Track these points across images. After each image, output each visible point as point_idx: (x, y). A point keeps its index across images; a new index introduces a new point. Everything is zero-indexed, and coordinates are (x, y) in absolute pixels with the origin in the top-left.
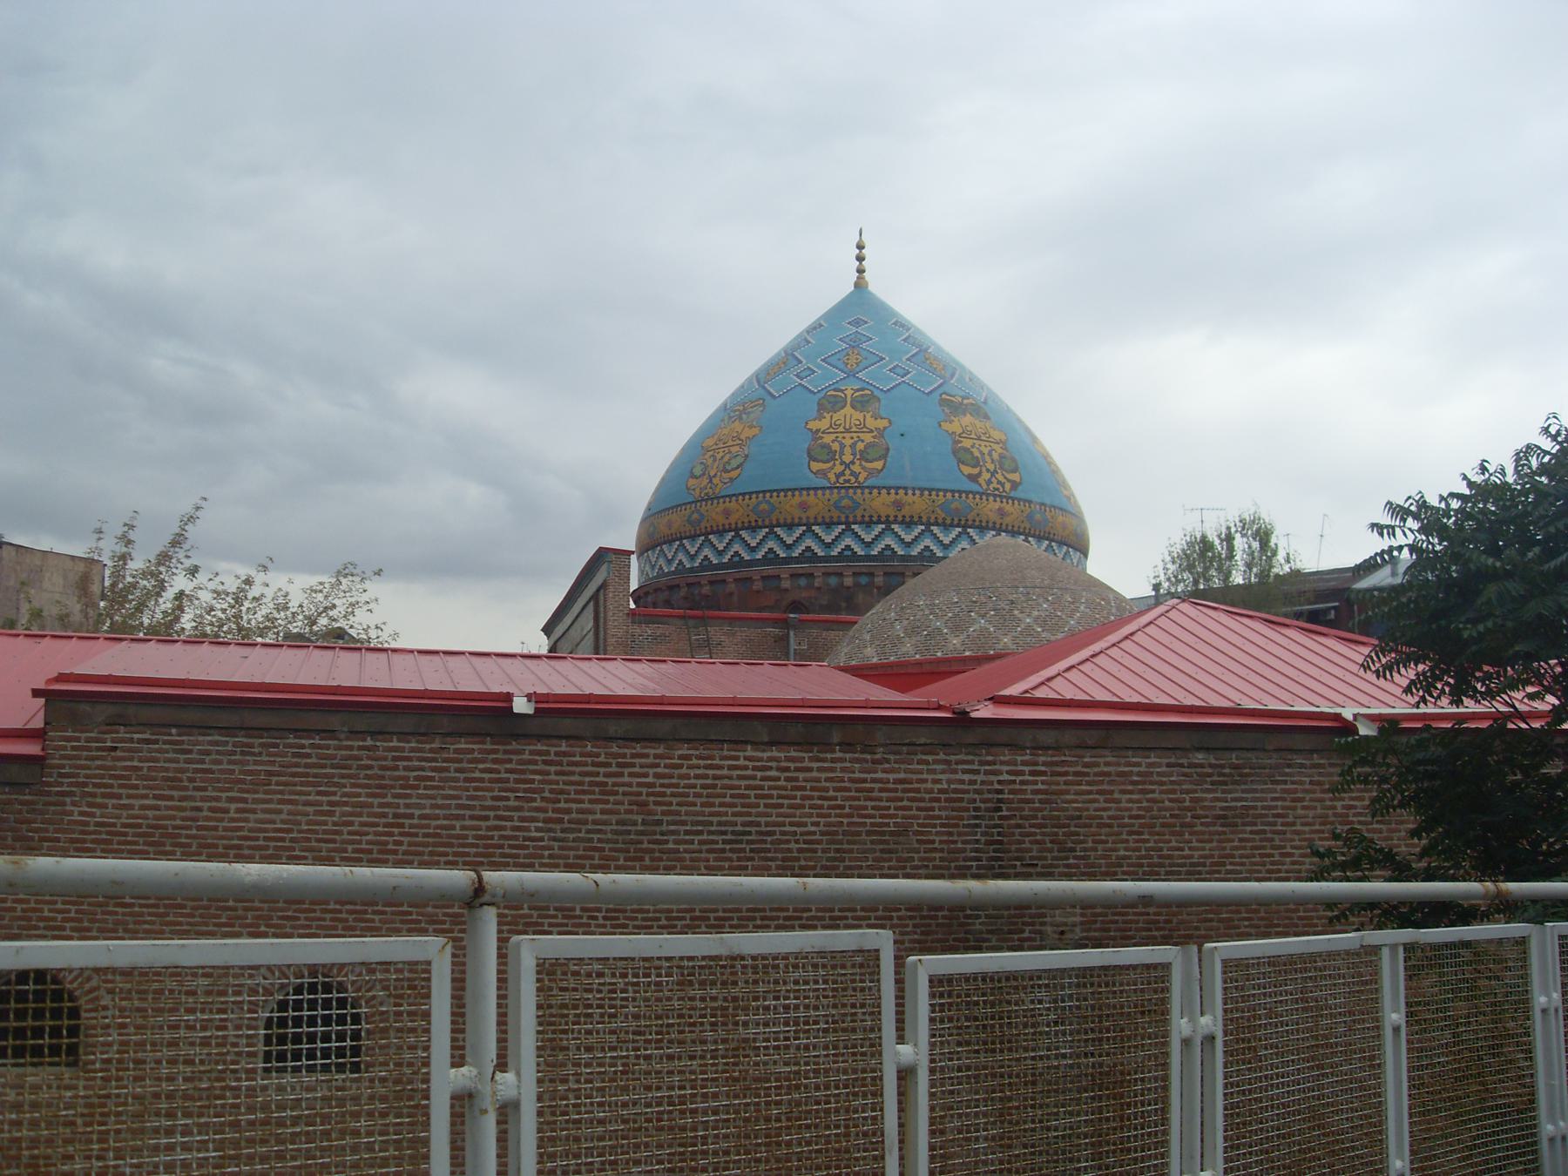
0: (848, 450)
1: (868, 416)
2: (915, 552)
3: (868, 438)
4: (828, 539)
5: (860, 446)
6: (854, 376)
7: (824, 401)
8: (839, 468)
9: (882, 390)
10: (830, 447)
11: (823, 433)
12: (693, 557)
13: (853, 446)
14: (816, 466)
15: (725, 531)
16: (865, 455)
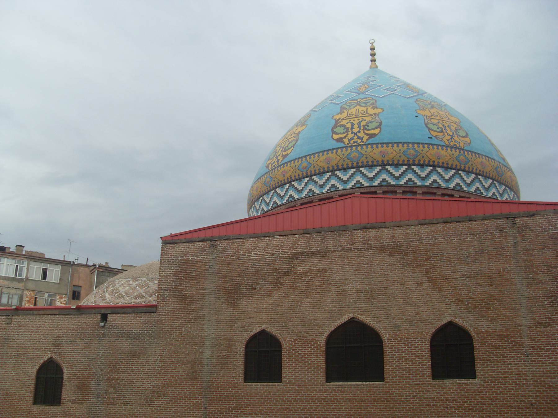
0: (356, 126)
1: (369, 109)
2: (402, 182)
3: (368, 119)
4: (345, 178)
5: (363, 123)
6: (363, 93)
7: (345, 106)
8: (350, 136)
9: (379, 97)
10: (346, 126)
11: (341, 120)
12: (268, 204)
13: (360, 123)
14: (335, 137)
15: (285, 184)
16: (366, 127)
